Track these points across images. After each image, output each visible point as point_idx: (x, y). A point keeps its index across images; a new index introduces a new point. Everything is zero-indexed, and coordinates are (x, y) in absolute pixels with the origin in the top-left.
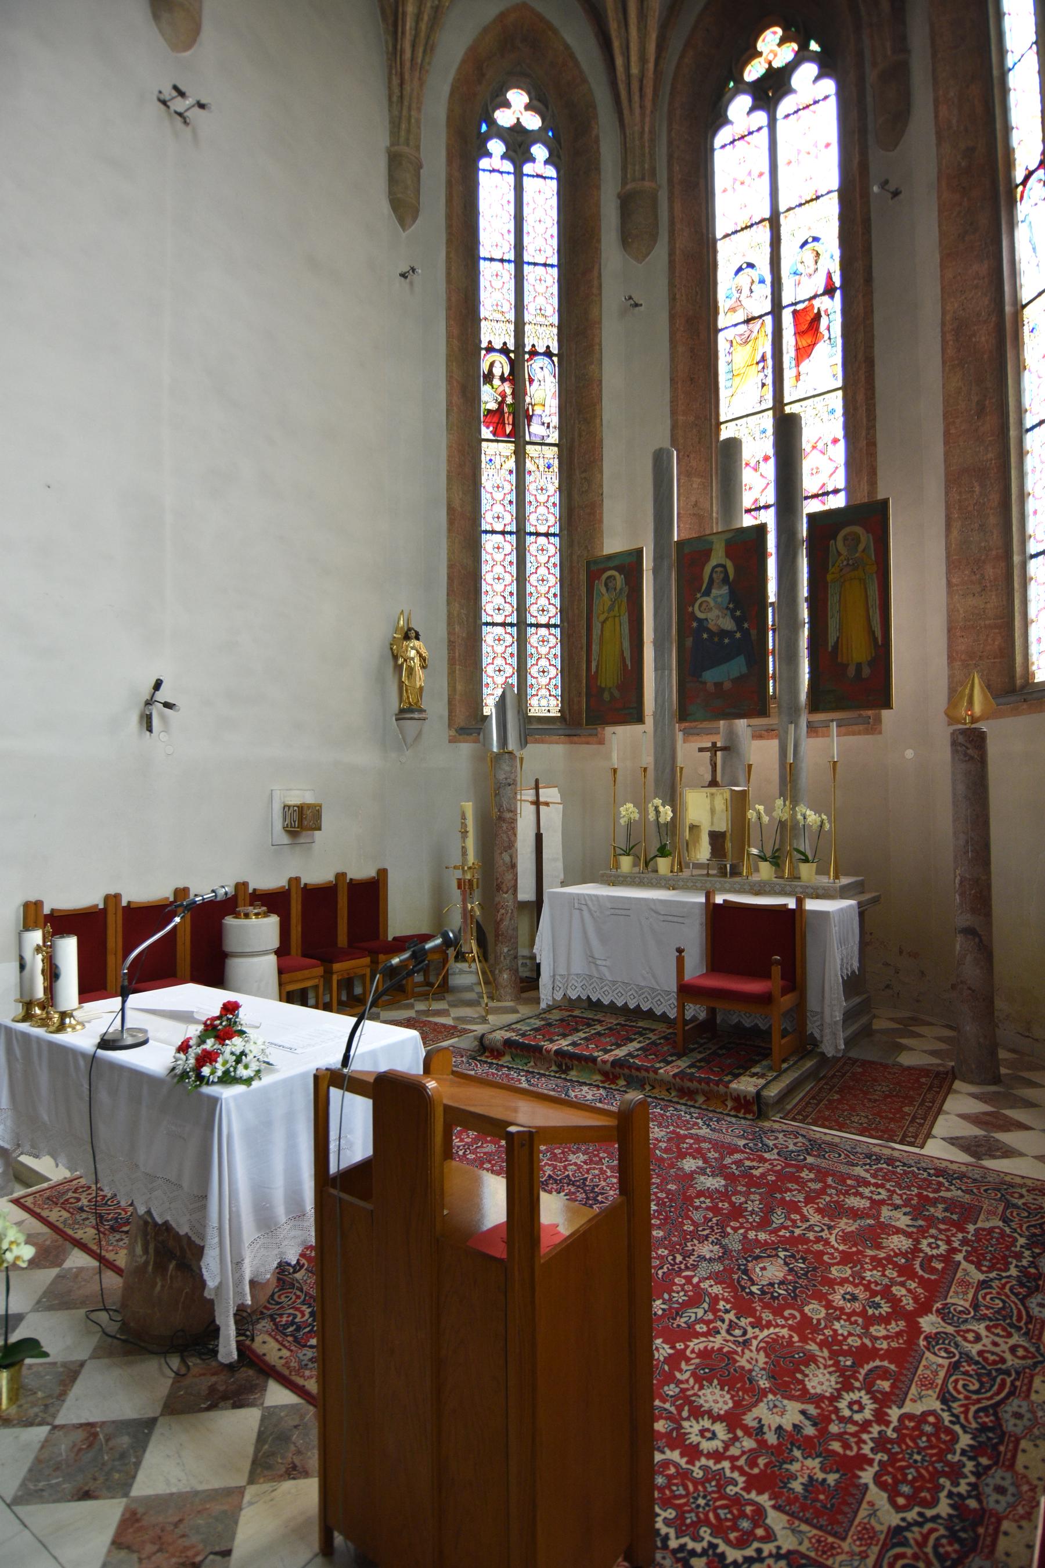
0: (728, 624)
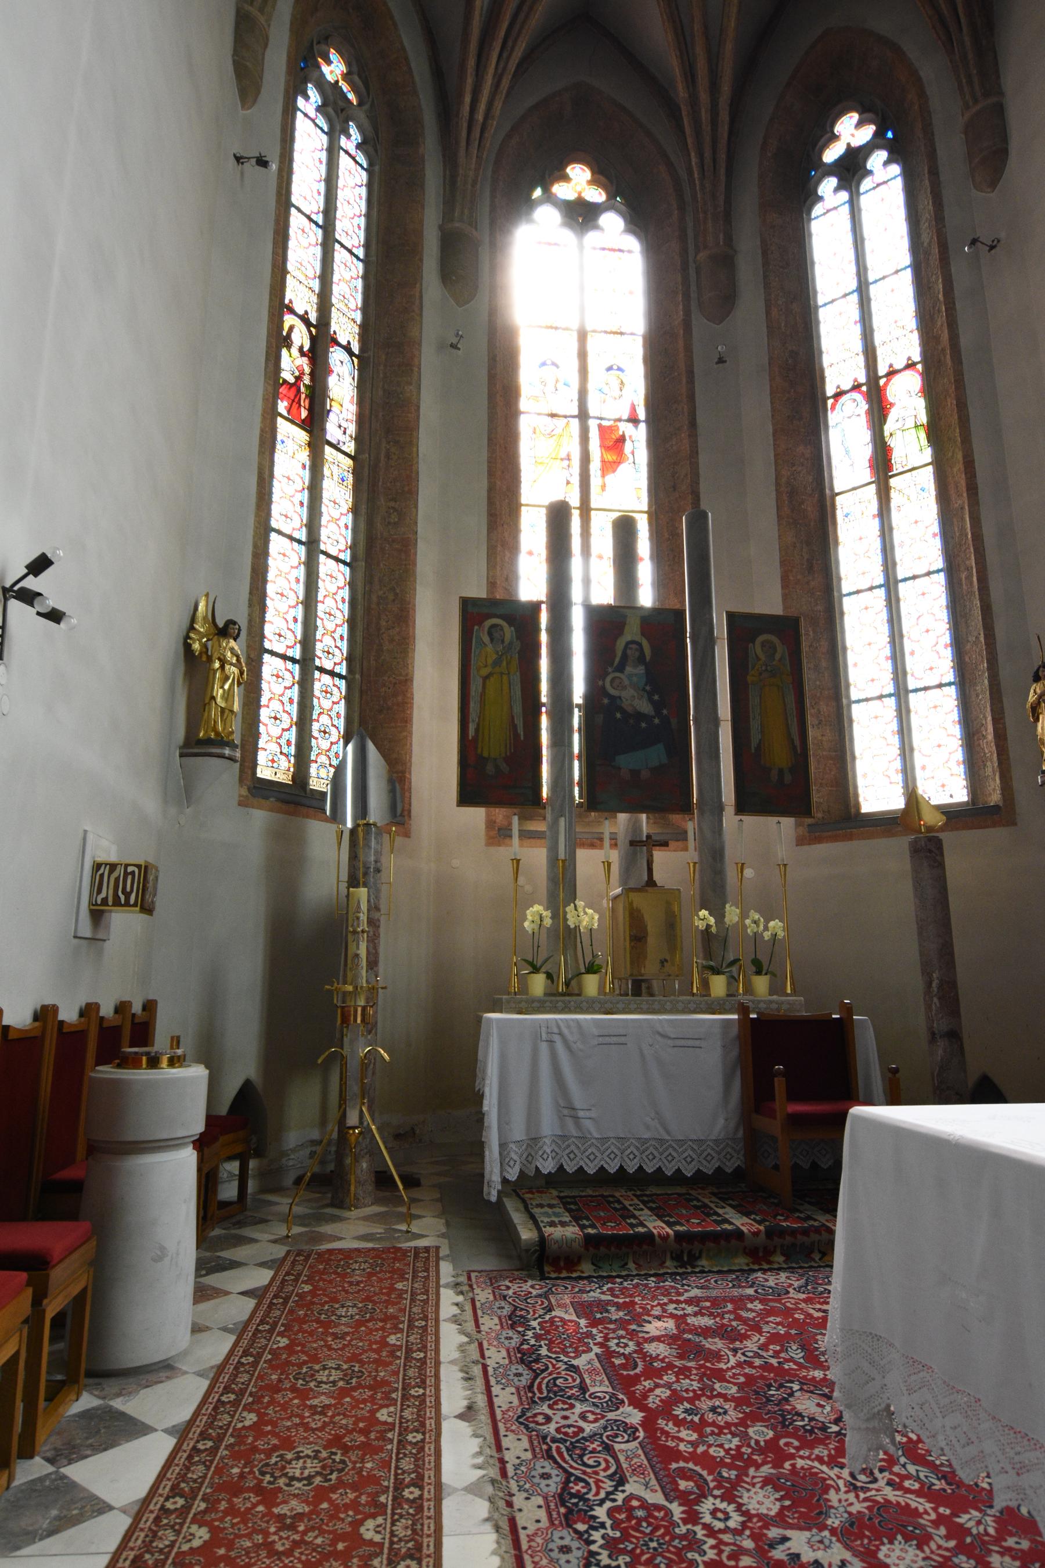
0: (645, 707)
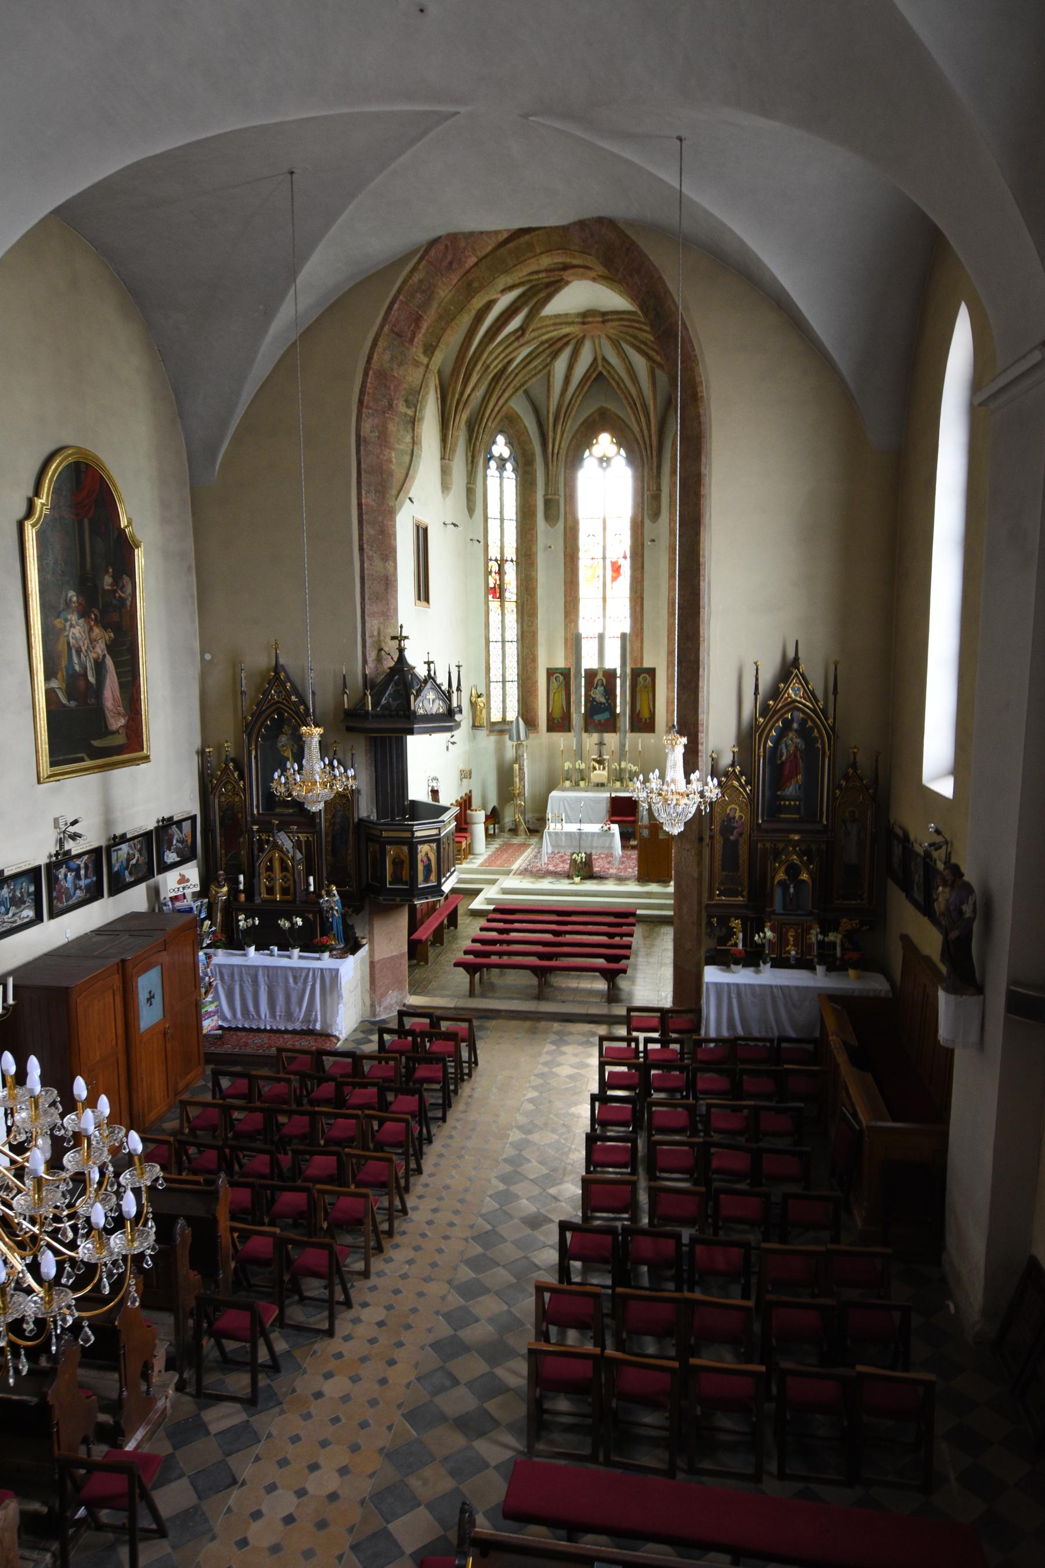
0: (603, 700)
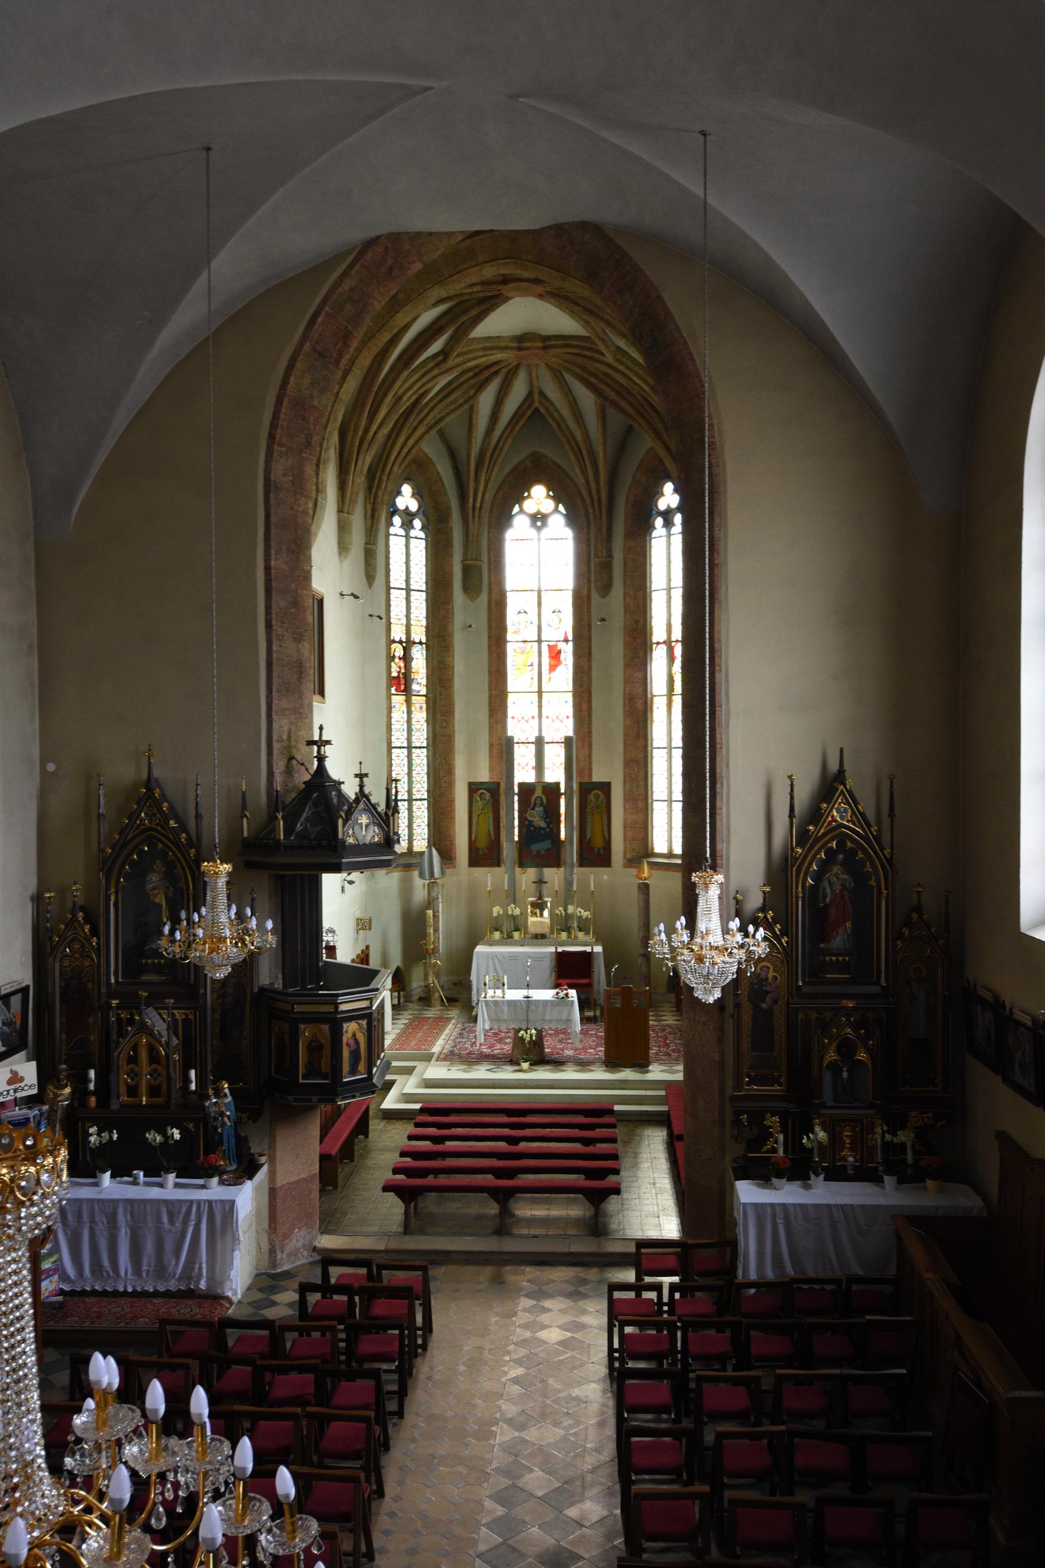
0: (543, 824)
